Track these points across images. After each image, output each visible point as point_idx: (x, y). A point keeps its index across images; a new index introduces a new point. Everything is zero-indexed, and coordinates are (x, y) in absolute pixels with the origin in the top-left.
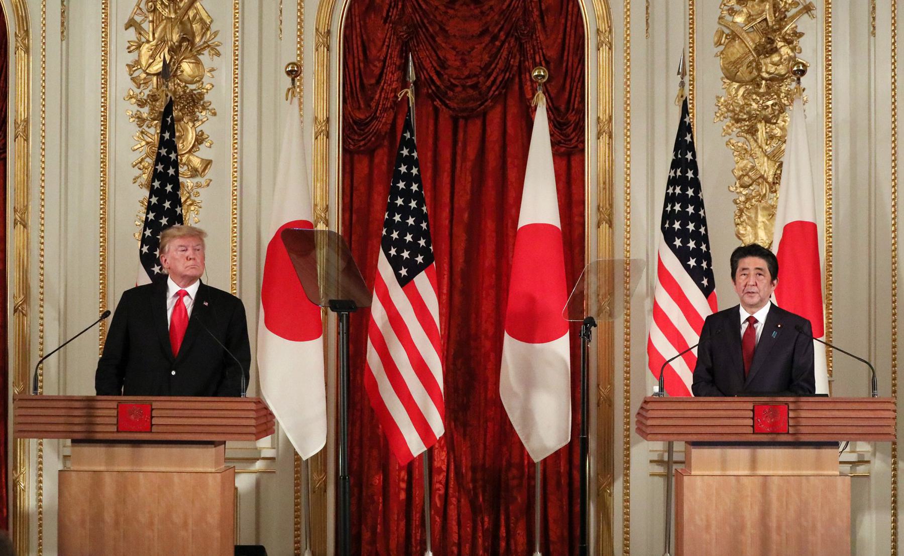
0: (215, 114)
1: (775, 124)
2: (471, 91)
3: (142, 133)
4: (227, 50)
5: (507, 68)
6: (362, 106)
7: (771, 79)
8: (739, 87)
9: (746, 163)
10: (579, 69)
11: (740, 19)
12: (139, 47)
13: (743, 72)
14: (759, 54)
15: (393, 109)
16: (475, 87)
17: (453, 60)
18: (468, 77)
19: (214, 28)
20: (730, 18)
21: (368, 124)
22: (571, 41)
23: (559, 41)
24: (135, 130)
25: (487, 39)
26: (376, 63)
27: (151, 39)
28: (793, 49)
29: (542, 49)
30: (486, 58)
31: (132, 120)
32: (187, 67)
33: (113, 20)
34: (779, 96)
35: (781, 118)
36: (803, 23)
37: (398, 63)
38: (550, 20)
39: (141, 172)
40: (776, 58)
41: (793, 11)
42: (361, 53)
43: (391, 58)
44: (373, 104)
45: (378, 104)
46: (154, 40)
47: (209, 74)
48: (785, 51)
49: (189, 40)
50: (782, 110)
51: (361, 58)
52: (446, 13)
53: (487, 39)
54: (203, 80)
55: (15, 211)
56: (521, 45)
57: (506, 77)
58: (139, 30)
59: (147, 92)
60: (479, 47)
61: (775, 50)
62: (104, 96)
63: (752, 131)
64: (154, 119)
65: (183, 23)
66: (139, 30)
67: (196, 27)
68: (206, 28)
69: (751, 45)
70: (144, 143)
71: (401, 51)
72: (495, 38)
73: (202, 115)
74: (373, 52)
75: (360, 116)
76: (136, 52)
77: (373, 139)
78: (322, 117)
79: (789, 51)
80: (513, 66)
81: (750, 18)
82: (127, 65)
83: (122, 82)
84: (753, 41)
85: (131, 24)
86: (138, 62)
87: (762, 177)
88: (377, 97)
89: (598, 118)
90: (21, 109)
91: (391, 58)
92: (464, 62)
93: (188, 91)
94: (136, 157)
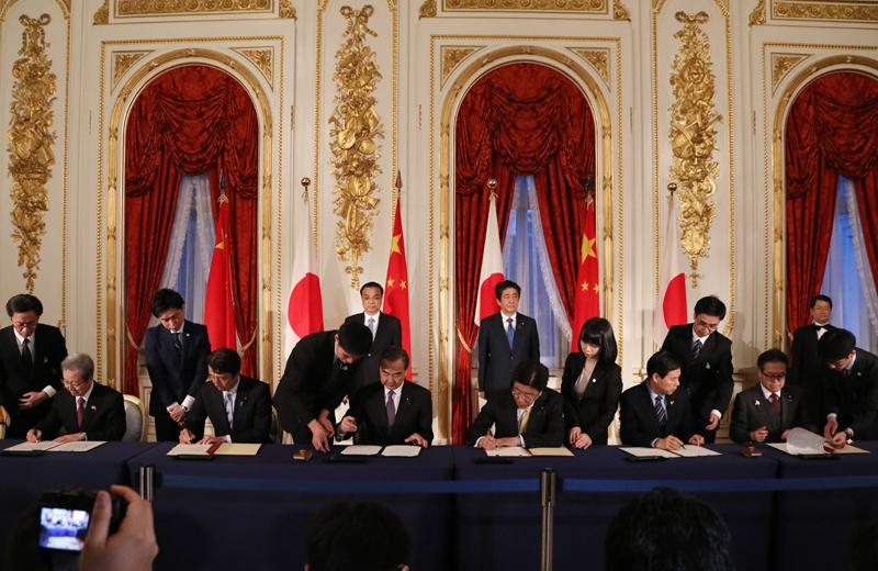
2: (530, 161)
5: (552, 147)
9: (687, 204)
11: (683, 123)
12: (337, 133)
13: (685, 153)
16: (533, 158)
17: (520, 143)
18: (530, 152)
19: (380, 123)
20: (676, 122)
24: (335, 182)
25: (540, 131)
32: (365, 145)
33: (321, 118)
38: (575, 120)
40: (702, 145)
41: (711, 119)
44: (475, 168)
48: (707, 141)
50: (706, 175)
52: (516, 115)
53: (540, 131)
55: (264, 229)
58: (337, 124)
60: (535, 136)
61: (702, 141)
62: (317, 161)
63: (690, 186)
66: (337, 124)
67: (371, 122)
68: (376, 122)
69: (689, 138)
72: (545, 131)
73: (374, 173)
74: (474, 137)
75: (468, 175)
78: (445, 175)
81: (688, 123)
83: (327, 155)
86: (336, 142)
87: (696, 212)
92: (527, 143)
94: (336, 197)
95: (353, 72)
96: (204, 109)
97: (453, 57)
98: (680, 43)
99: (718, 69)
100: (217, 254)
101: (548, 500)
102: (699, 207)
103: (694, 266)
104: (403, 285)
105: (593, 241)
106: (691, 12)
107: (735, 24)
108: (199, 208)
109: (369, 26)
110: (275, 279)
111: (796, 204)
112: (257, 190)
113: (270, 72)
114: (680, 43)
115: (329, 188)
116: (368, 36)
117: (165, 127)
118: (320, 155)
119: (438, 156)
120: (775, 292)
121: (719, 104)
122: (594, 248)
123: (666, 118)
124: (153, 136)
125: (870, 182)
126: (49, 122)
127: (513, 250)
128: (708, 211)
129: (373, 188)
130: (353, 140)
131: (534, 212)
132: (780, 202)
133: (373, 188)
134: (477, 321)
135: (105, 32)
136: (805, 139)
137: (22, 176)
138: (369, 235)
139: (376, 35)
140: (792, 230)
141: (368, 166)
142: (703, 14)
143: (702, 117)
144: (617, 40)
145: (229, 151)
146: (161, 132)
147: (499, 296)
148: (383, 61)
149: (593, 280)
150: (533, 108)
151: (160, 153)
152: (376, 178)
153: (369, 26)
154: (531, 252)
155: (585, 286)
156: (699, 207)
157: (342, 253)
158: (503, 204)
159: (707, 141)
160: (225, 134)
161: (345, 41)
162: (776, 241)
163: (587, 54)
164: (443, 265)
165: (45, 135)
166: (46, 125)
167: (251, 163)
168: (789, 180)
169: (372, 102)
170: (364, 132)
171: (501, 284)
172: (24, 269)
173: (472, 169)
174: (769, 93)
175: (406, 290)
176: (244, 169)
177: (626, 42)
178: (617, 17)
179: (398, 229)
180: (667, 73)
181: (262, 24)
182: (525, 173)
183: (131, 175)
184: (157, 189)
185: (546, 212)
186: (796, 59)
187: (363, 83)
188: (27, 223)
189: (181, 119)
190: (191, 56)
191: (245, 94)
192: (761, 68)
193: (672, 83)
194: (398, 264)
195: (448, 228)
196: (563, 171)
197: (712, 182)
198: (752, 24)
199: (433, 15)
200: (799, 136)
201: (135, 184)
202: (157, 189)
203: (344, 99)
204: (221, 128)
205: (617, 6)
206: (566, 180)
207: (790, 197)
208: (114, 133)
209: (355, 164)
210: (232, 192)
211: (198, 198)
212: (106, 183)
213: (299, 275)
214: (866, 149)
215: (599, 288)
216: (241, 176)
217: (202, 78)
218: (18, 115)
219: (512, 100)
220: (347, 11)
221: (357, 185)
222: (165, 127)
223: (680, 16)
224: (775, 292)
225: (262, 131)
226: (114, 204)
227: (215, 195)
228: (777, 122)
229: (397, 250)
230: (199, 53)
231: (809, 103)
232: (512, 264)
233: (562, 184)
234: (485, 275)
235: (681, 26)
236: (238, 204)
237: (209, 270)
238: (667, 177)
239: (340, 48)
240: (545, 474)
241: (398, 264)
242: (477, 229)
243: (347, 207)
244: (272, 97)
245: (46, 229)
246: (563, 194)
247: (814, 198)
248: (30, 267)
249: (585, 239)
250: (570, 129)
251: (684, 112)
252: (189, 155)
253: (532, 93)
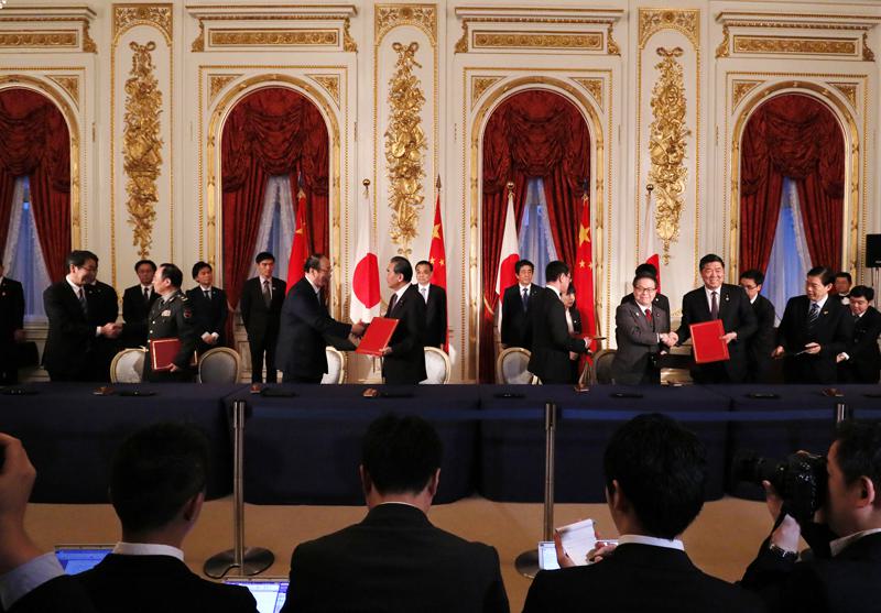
4: (431, 147)
5: (557, 157)
9: (662, 201)
11: (660, 137)
12: (391, 145)
16: (543, 165)
17: (532, 154)
22: (585, 145)
30: (548, 152)
36: (686, 139)
38: (575, 136)
48: (679, 151)
58: (391, 137)
61: (675, 151)
63: (665, 187)
65: (412, 135)
66: (391, 137)
67: (417, 136)
68: (421, 137)
73: (420, 176)
74: (497, 149)
81: (664, 137)
83: (383, 161)
85: (387, 134)
86: (390, 152)
90: (337, 172)
94: (390, 195)
95: (403, 96)
96: (285, 124)
97: (481, 85)
98: (659, 73)
99: (689, 94)
100: (297, 238)
101: (550, 425)
102: (671, 203)
103: (666, 248)
104: (442, 263)
105: (587, 230)
106: (669, 48)
107: (704, 55)
108: (283, 202)
109: (416, 59)
110: (343, 259)
113: (337, 95)
114: (659, 73)
115: (385, 187)
116: (414, 67)
117: (253, 137)
118: (378, 162)
119: (469, 164)
120: (730, 268)
121: (689, 121)
122: (589, 235)
123: (646, 133)
126: (157, 131)
127: (527, 237)
128: (678, 206)
129: (419, 188)
130: (403, 151)
131: (543, 208)
132: (736, 199)
133: (419, 188)
134: (498, 291)
135: (201, 58)
137: (136, 174)
138: (415, 224)
139: (420, 67)
140: (745, 220)
141: (415, 171)
142: (679, 49)
143: (676, 133)
144: (610, 71)
147: (518, 272)
148: (426, 88)
149: (588, 259)
150: (543, 126)
152: (421, 180)
153: (416, 59)
154: (539, 240)
155: (582, 264)
156: (671, 203)
157: (395, 238)
158: (519, 200)
159: (679, 151)
161: (396, 71)
163: (585, 82)
164: (473, 248)
165: (154, 141)
166: (155, 133)
169: (418, 120)
170: (412, 144)
171: (517, 263)
172: (139, 248)
174: (730, 113)
175: (444, 267)
177: (617, 74)
178: (610, 52)
179: (438, 220)
180: (648, 96)
181: (330, 55)
182: (536, 178)
183: (226, 175)
184: (247, 190)
185: (552, 207)
186: (752, 85)
187: (411, 105)
188: (140, 211)
189: (265, 130)
190: (273, 80)
191: (318, 112)
192: (724, 92)
193: (652, 105)
194: (438, 246)
195: (476, 220)
196: (565, 176)
197: (681, 183)
198: (718, 56)
199: (465, 51)
200: (753, 147)
201: (230, 182)
202: (247, 190)
203: (396, 118)
204: (298, 139)
205: (611, 43)
207: (744, 195)
208: (211, 140)
209: (405, 169)
210: (309, 190)
211: (281, 194)
212: (206, 181)
213: (361, 255)
214: (807, 157)
215: (592, 265)
216: (315, 177)
217: (283, 98)
218: (130, 124)
219: (526, 120)
220: (397, 47)
221: (406, 186)
222: (253, 137)
223: (660, 51)
224: (730, 268)
225: (331, 142)
226: (213, 197)
227: (295, 192)
228: (735, 135)
229: (437, 236)
230: (280, 78)
231: (762, 120)
232: (526, 248)
233: (565, 185)
234: (504, 255)
235: (661, 59)
236: (314, 198)
237: (290, 251)
238: (646, 180)
239: (392, 77)
240: (548, 406)
241: (438, 246)
242: (499, 220)
243: (399, 202)
244: (340, 115)
245: (156, 216)
246: (566, 193)
247: (764, 195)
248: (143, 246)
249: (582, 228)
250: (571, 142)
251: (661, 128)
253: (542, 115)
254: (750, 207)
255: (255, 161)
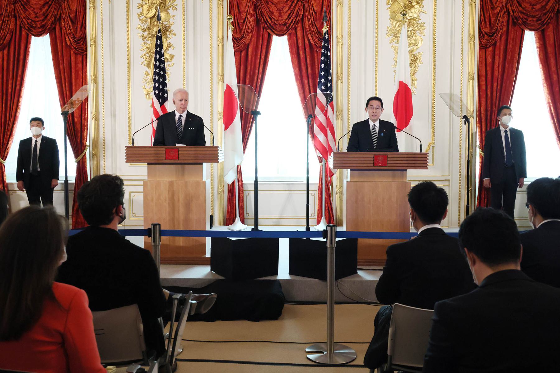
0: (175, 35)
1: (411, 38)
3: (144, 43)
4: (180, 7)
6: (238, 32)
7: (410, 19)
8: (397, 23)
10: (329, 15)
12: (142, 6)
14: (405, 8)
15: (251, 33)
21: (240, 40)
23: (321, 3)
26: (244, 13)
27: (147, 3)
28: (420, 6)
29: (313, 7)
31: (140, 38)
32: (163, 15)
34: (414, 27)
35: (414, 36)
37: (253, 14)
39: (144, 60)
40: (413, 10)
42: (237, 10)
43: (250, 11)
45: (245, 30)
46: (148, 3)
47: (172, 18)
49: (163, 3)
51: (237, 11)
54: (170, 21)
55: (91, 76)
56: (304, 5)
57: (297, 19)
59: (146, 26)
61: (413, 6)
64: (149, 37)
69: (402, 4)
70: (145, 47)
71: (254, 8)
74: (242, 9)
76: (141, 8)
77: (243, 46)
78: (220, 37)
79: (418, 7)
80: (300, 15)
82: (138, 14)
83: (135, 22)
84: (403, 3)
86: (142, 13)
88: (244, 28)
89: (337, 36)
91: (250, 11)
93: (163, 25)
94: (143, 53)
111: (488, 53)
112: (86, 48)
118: (131, 21)
124: (7, 6)
125: (550, 33)
129: (169, 46)
130: (153, 12)
136: (496, 3)
145: (64, 19)
146: (14, 4)
151: (13, 19)
160: (61, 6)
162: (469, 81)
167: (81, 28)
168: (482, 35)
173: (240, 32)
176: (77, 33)
206: (309, 40)
207: (482, 47)
214: (548, 7)
233: (307, 42)
246: (308, 50)
252: (35, 22)
254: (489, 60)
255: (18, 23)
